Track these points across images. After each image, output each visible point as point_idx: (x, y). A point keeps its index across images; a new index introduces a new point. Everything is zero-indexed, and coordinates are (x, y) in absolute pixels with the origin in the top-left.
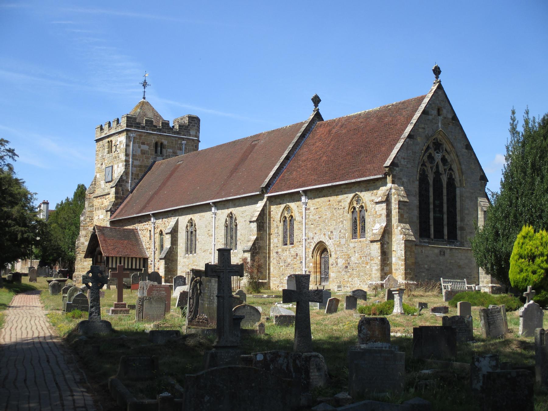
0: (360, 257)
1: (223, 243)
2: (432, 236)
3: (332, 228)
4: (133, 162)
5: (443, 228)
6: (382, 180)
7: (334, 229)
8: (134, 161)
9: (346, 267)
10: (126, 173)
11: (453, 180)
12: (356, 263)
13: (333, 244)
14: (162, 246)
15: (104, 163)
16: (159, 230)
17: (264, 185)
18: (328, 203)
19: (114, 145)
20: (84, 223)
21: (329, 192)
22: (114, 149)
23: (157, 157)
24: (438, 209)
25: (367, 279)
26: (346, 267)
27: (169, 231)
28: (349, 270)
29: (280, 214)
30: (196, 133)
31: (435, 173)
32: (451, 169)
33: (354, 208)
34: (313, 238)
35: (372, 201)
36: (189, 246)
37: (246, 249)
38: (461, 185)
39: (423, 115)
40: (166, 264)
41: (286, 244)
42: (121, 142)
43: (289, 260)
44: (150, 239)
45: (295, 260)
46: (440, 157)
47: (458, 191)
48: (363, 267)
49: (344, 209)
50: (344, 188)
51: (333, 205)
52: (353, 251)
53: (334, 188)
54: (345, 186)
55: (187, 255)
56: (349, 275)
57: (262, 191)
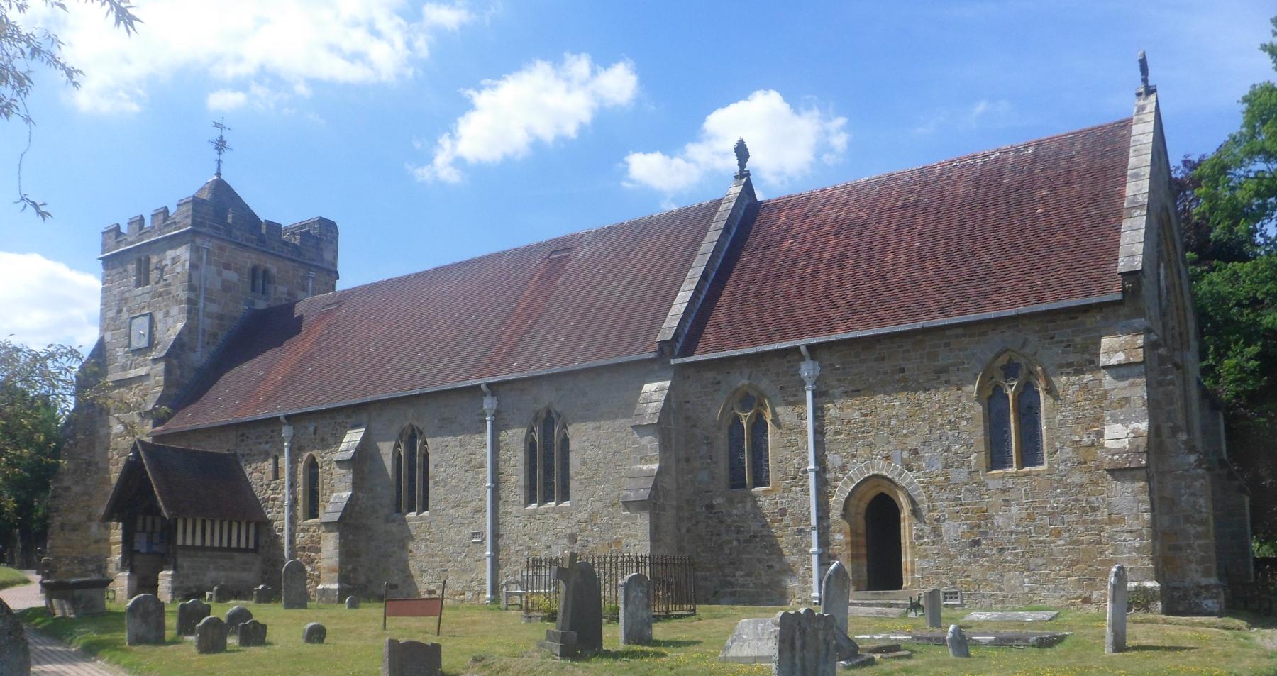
0: (1031, 517)
1: (522, 483)
3: (913, 442)
6: (1104, 310)
7: (924, 444)
8: (208, 303)
9: (976, 543)
10: (188, 329)
12: (1011, 533)
15: (125, 309)
18: (897, 377)
19: (157, 268)
20: (71, 442)
21: (901, 346)
22: (154, 275)
23: (256, 301)
25: (1057, 574)
27: (349, 455)
28: (987, 552)
34: (843, 469)
37: (632, 496)
38: (1182, 345)
42: (177, 260)
44: (276, 477)
48: (1040, 542)
50: (957, 336)
53: (920, 337)
54: (960, 331)
57: (661, 349)
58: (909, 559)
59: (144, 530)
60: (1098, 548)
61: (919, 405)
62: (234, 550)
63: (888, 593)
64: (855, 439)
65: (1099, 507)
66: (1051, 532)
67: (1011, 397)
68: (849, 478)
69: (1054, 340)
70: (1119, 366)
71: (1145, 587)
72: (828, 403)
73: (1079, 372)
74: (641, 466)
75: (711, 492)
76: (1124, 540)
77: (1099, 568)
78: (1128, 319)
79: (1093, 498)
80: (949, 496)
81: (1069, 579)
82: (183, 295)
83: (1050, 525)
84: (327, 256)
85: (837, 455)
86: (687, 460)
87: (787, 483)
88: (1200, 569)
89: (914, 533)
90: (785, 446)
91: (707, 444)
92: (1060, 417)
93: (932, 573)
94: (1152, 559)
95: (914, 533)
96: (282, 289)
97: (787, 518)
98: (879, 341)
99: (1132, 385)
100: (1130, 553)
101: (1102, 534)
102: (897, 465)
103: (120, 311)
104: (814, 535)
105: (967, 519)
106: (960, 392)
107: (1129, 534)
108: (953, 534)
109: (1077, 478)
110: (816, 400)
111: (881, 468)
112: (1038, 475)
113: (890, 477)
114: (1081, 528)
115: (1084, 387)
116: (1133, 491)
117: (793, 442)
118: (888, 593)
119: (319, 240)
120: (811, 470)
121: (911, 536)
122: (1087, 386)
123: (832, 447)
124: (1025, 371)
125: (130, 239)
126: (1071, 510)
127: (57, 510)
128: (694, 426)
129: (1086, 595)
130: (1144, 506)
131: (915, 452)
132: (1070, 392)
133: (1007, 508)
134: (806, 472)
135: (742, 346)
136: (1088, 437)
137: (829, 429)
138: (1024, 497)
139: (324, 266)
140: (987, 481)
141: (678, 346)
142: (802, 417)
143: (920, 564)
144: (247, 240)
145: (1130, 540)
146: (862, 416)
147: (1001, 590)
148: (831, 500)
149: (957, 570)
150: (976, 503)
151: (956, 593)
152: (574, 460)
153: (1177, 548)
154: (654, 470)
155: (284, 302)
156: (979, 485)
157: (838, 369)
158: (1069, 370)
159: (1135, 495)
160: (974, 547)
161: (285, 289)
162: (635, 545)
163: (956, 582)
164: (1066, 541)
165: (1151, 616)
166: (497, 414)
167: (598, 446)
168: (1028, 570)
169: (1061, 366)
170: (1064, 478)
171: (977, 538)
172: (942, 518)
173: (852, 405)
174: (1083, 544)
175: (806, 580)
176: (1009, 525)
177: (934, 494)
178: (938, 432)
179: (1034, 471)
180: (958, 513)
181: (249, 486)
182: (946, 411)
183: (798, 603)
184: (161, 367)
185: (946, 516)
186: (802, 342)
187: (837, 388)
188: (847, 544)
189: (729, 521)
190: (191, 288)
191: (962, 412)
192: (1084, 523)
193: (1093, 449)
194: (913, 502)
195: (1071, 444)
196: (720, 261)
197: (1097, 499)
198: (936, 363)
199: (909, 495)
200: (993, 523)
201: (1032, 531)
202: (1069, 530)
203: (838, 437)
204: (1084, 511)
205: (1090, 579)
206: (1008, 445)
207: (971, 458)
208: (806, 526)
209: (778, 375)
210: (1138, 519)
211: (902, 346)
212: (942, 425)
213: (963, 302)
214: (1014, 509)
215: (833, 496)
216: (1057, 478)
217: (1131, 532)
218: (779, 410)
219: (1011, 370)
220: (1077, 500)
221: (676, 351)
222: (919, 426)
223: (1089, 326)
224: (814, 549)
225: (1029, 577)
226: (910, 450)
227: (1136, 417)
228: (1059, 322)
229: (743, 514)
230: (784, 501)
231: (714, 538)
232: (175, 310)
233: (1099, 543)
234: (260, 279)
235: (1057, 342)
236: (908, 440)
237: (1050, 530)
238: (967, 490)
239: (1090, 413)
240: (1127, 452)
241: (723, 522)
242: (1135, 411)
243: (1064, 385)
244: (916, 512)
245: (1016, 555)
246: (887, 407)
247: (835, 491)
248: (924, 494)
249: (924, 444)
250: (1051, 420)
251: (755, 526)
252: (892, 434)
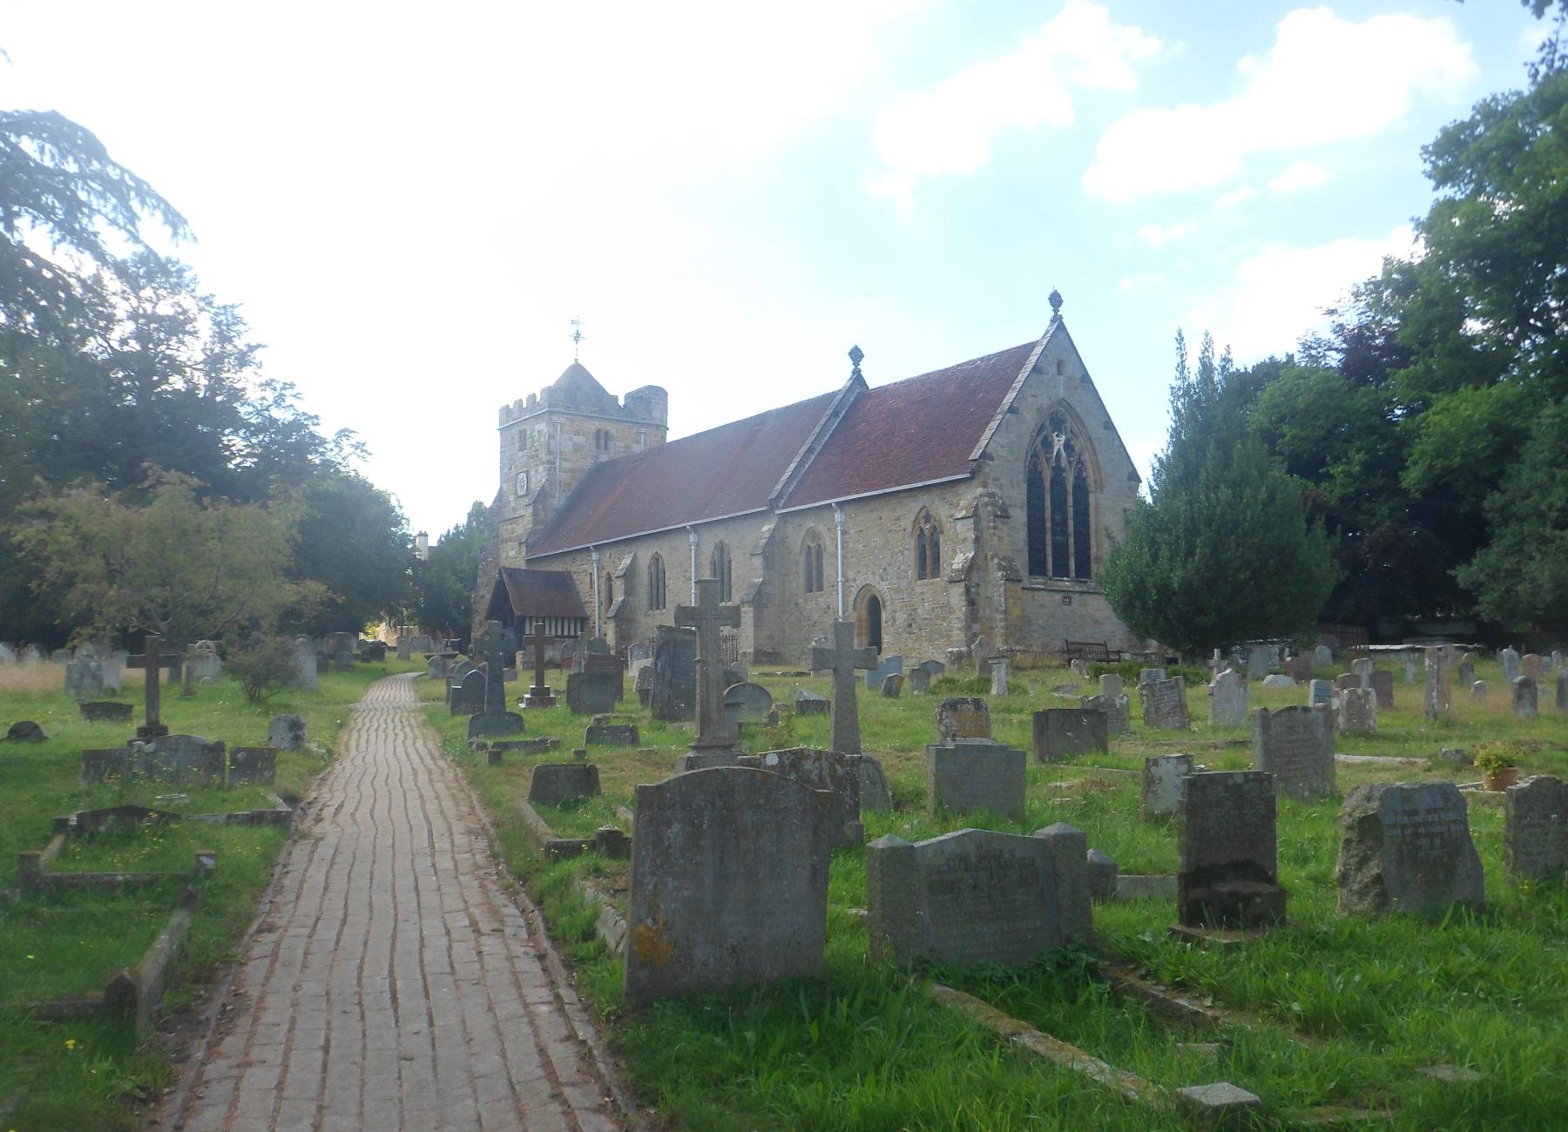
0: (933, 609)
2: (1050, 573)
4: (560, 464)
5: (1068, 559)
9: (910, 625)
10: (550, 481)
11: (1084, 479)
12: (925, 619)
14: (610, 599)
16: (605, 572)
17: (773, 496)
22: (529, 442)
24: (1059, 529)
26: (910, 625)
29: (799, 544)
30: (662, 415)
31: (1053, 468)
32: (1080, 462)
33: (922, 530)
34: (854, 580)
35: (952, 516)
36: (654, 598)
38: (1096, 488)
39: (1034, 375)
40: (617, 626)
41: (811, 591)
43: (816, 616)
46: (1062, 442)
47: (1092, 498)
50: (905, 498)
54: (906, 494)
55: (650, 612)
59: (512, 625)
62: (567, 637)
82: (545, 457)
84: (656, 414)
96: (620, 444)
97: (831, 611)
99: (968, 530)
103: (510, 469)
119: (649, 403)
125: (515, 416)
127: (477, 611)
139: (654, 422)
141: (783, 501)
144: (591, 412)
152: (734, 575)
153: (992, 628)
155: (623, 454)
161: (623, 444)
166: (698, 545)
181: (578, 593)
184: (530, 509)
190: (550, 452)
194: (884, 602)
196: (826, 438)
221: (780, 505)
232: (541, 469)
234: (603, 439)
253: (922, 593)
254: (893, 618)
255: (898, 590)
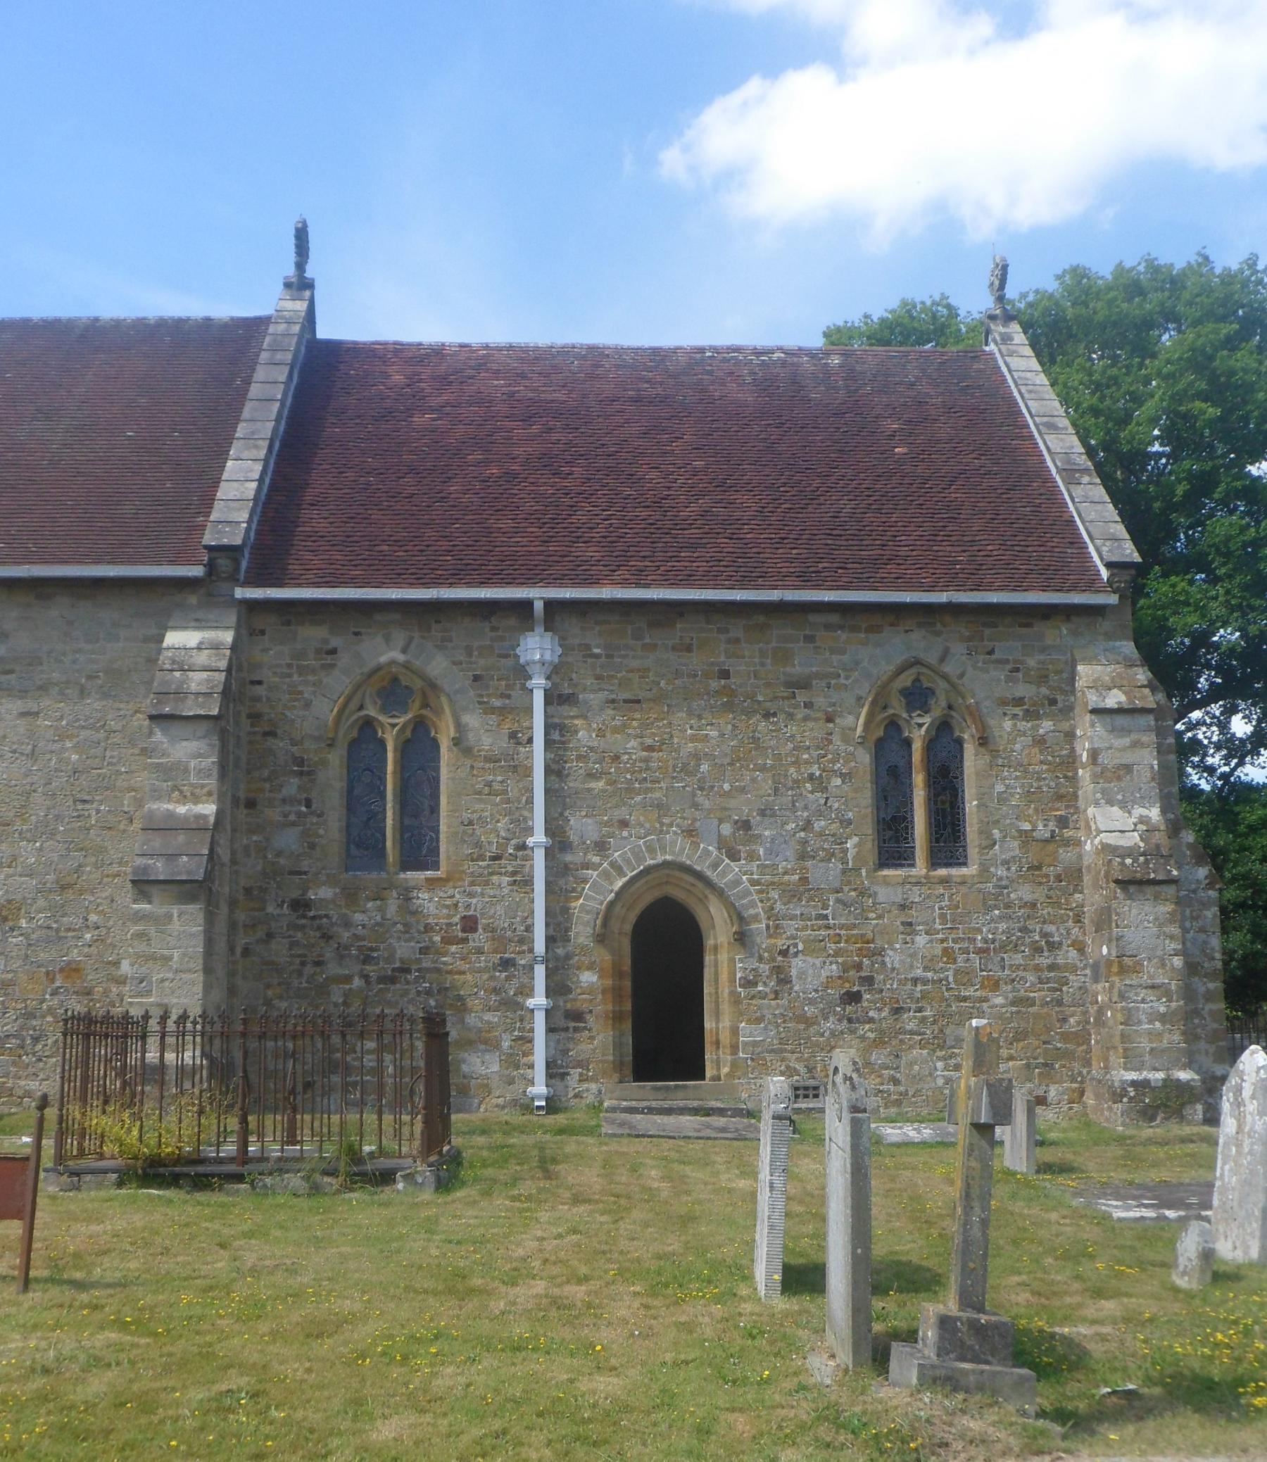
3: (743, 807)
9: (854, 998)
12: (915, 981)
13: (754, 883)
18: (714, 684)
28: (871, 1014)
34: (601, 847)
45: (453, 948)
48: (965, 999)
49: (829, 720)
50: (828, 627)
51: (752, 697)
52: (894, 920)
53: (761, 619)
54: (834, 618)
56: (871, 1035)
58: (726, 1023)
60: (1057, 1012)
61: (755, 740)
63: (685, 1087)
64: (630, 790)
65: (1060, 943)
66: (982, 983)
67: (917, 747)
68: (612, 864)
69: (994, 657)
70: (1120, 711)
71: (1178, 1080)
72: (574, 717)
73: (1031, 715)
74: (170, 807)
75: (305, 873)
76: (1143, 1001)
77: (1059, 1045)
78: (1110, 639)
79: (1051, 928)
80: (806, 911)
81: (1011, 1063)
83: (982, 970)
85: (589, 821)
86: (251, 804)
87: (480, 867)
88: (1212, 1049)
89: (739, 975)
90: (480, 793)
91: (301, 773)
92: (1000, 788)
93: (772, 1051)
94: (1184, 1033)
95: (739, 975)
97: (480, 938)
98: (681, 615)
99: (1135, 745)
100: (1151, 1022)
101: (1065, 988)
102: (710, 848)
104: (540, 971)
105: (837, 953)
106: (831, 725)
107: (1150, 991)
108: (812, 982)
109: (1025, 892)
110: (550, 709)
111: (677, 849)
112: (963, 883)
113: (698, 868)
114: (1031, 978)
115: (1040, 742)
116: (1156, 919)
117: (496, 786)
118: (685, 1087)
120: (538, 845)
121: (732, 980)
122: (1045, 740)
123: (579, 803)
124: (944, 704)
126: (1016, 946)
128: (272, 734)
129: (1041, 1093)
130: (1172, 946)
131: (746, 825)
132: (1018, 747)
133: (908, 939)
134: (523, 847)
135: (397, 585)
136: (1045, 826)
137: (575, 767)
138: (937, 920)
140: (876, 888)
142: (520, 738)
143: (749, 1033)
145: (1152, 1001)
146: (643, 750)
147: (896, 1082)
148: (573, 904)
149: (817, 1044)
150: (854, 926)
151: (816, 1088)
154: (205, 817)
156: (862, 894)
157: (597, 656)
158: (1017, 710)
159: (1160, 926)
160: (850, 1004)
162: (163, 981)
163: (815, 1068)
164: (1006, 998)
165: (1187, 1130)
167: (32, 755)
168: (941, 1048)
169: (1003, 702)
170: (1006, 891)
171: (856, 989)
172: (792, 950)
173: (624, 726)
174: (1033, 1005)
175: (516, 1061)
176: (912, 966)
177: (778, 906)
178: (790, 793)
179: (956, 876)
180: (822, 941)
182: (805, 756)
183: (497, 1106)
185: (801, 947)
186: (537, 594)
187: (595, 691)
188: (604, 992)
189: (346, 935)
191: (833, 761)
192: (1037, 968)
193: (1051, 847)
195: (1016, 834)
197: (1058, 929)
198: (788, 669)
199: (733, 904)
200: (883, 963)
201: (951, 979)
202: (1013, 980)
203: (592, 785)
204: (1038, 950)
205: (1046, 1065)
206: (907, 828)
207: (848, 845)
208: (519, 953)
209: (469, 651)
210: (1163, 965)
211: (727, 631)
212: (796, 781)
213: (841, 568)
214: (921, 940)
215: (578, 898)
216: (993, 891)
217: (1153, 987)
218: (467, 719)
219: (917, 697)
220: (1024, 930)
222: (754, 780)
223: (1049, 642)
224: (538, 1000)
225: (944, 1059)
226: (736, 822)
227: (1141, 797)
228: (1001, 628)
229: (377, 924)
230: (474, 901)
231: (309, 970)
233: (1059, 1003)
235: (999, 662)
236: (733, 803)
237: (979, 979)
238: (838, 901)
239: (1048, 785)
240: (1144, 854)
241: (330, 937)
242: (1140, 789)
243: (1009, 734)
244: (742, 938)
245: (924, 1019)
246: (693, 739)
247: (584, 888)
248: (759, 904)
249: (762, 813)
250: (986, 790)
251: (404, 950)
252: (701, 789)
253: (903, 907)
254: (778, 970)
255: (800, 890)
